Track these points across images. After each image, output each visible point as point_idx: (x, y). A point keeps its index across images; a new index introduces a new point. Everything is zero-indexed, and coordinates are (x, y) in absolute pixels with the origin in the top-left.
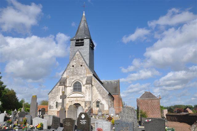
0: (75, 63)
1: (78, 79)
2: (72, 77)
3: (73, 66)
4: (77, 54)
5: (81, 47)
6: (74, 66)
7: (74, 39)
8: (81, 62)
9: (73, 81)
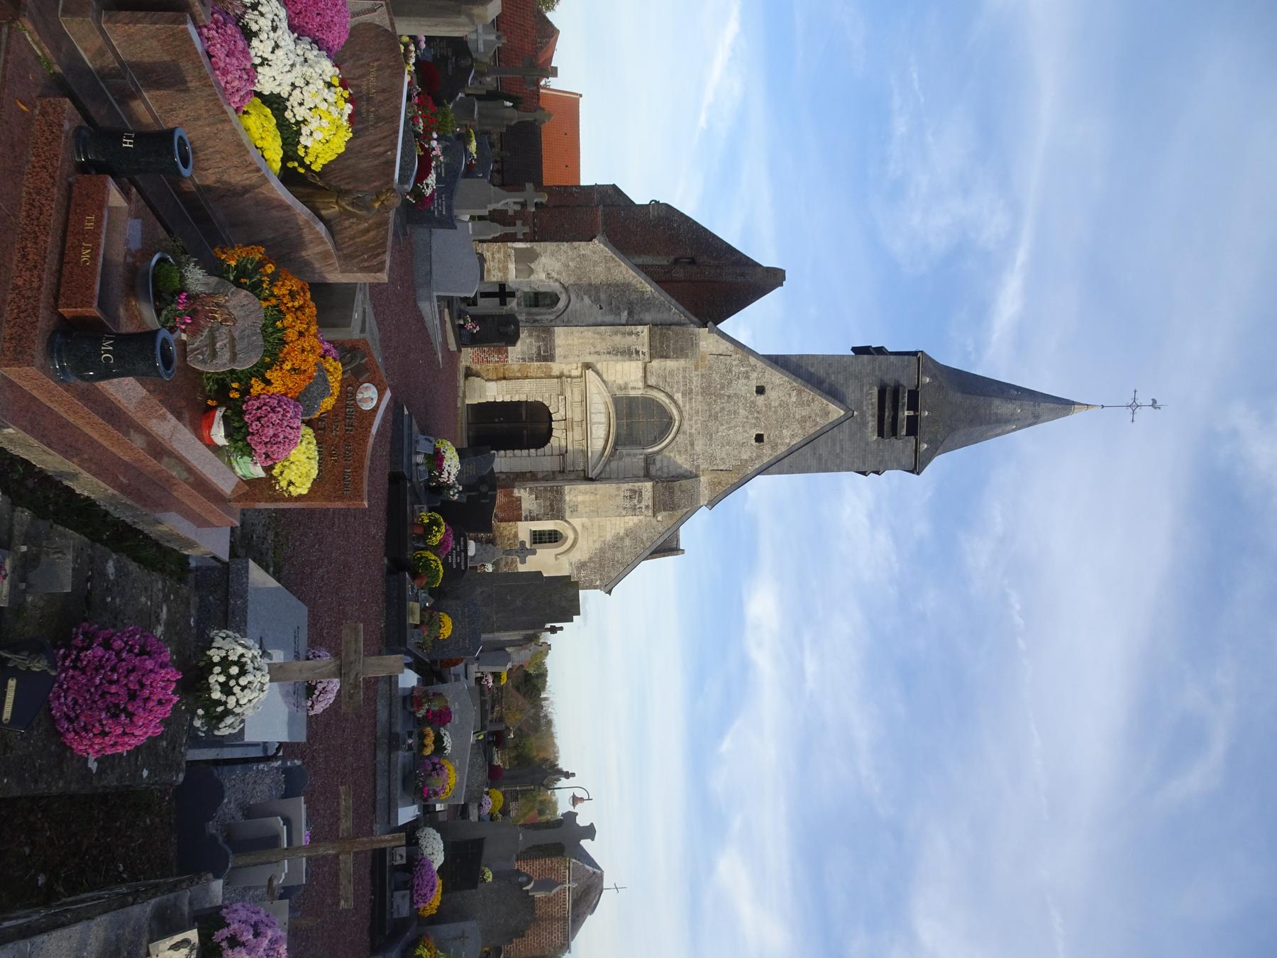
1: (686, 426)
2: (696, 383)
3: (760, 390)
4: (832, 407)
5: (872, 423)
6: (760, 400)
8: (781, 437)
9: (678, 396)
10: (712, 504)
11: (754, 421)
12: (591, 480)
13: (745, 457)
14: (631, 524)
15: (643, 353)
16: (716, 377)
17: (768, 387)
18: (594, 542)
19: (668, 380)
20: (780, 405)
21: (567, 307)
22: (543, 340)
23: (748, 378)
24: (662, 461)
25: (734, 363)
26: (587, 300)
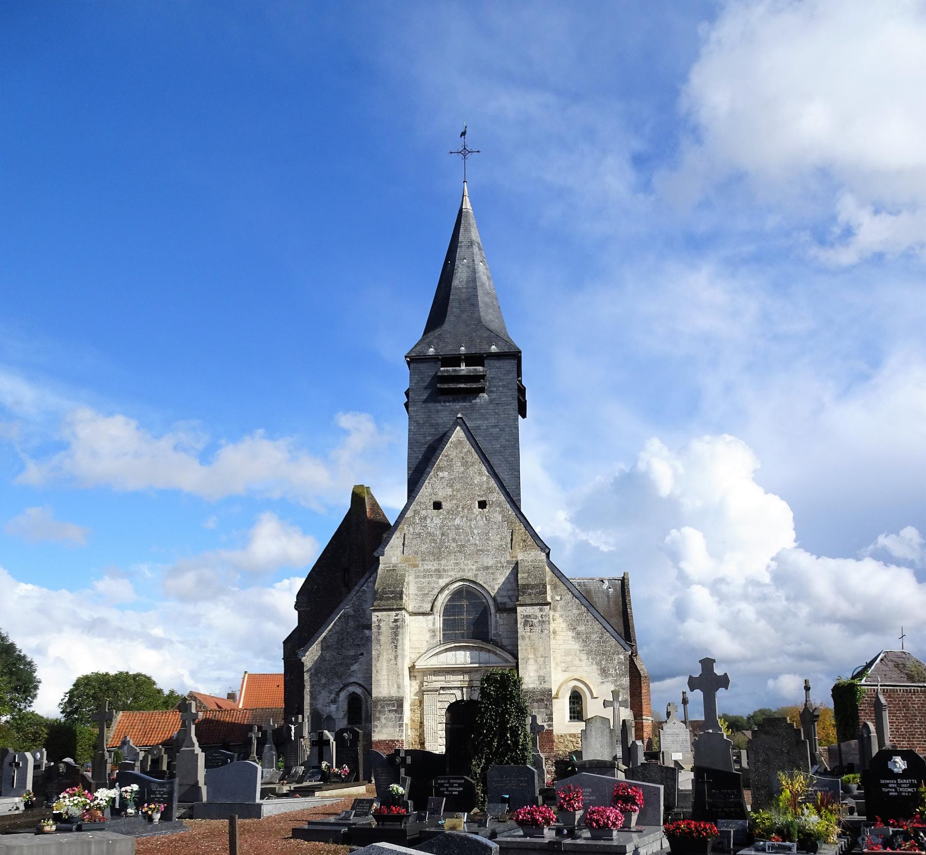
0: (449, 491)
2: (431, 565)
3: (437, 506)
4: (453, 438)
7: (431, 351)
8: (480, 485)
9: (442, 582)
11: (466, 511)
14: (564, 625)
15: (397, 615)
17: (435, 499)
18: (580, 660)
19: (426, 592)
20: (451, 486)
21: (360, 685)
22: (383, 707)
23: (425, 518)
24: (502, 596)
25: (412, 530)
26: (355, 667)
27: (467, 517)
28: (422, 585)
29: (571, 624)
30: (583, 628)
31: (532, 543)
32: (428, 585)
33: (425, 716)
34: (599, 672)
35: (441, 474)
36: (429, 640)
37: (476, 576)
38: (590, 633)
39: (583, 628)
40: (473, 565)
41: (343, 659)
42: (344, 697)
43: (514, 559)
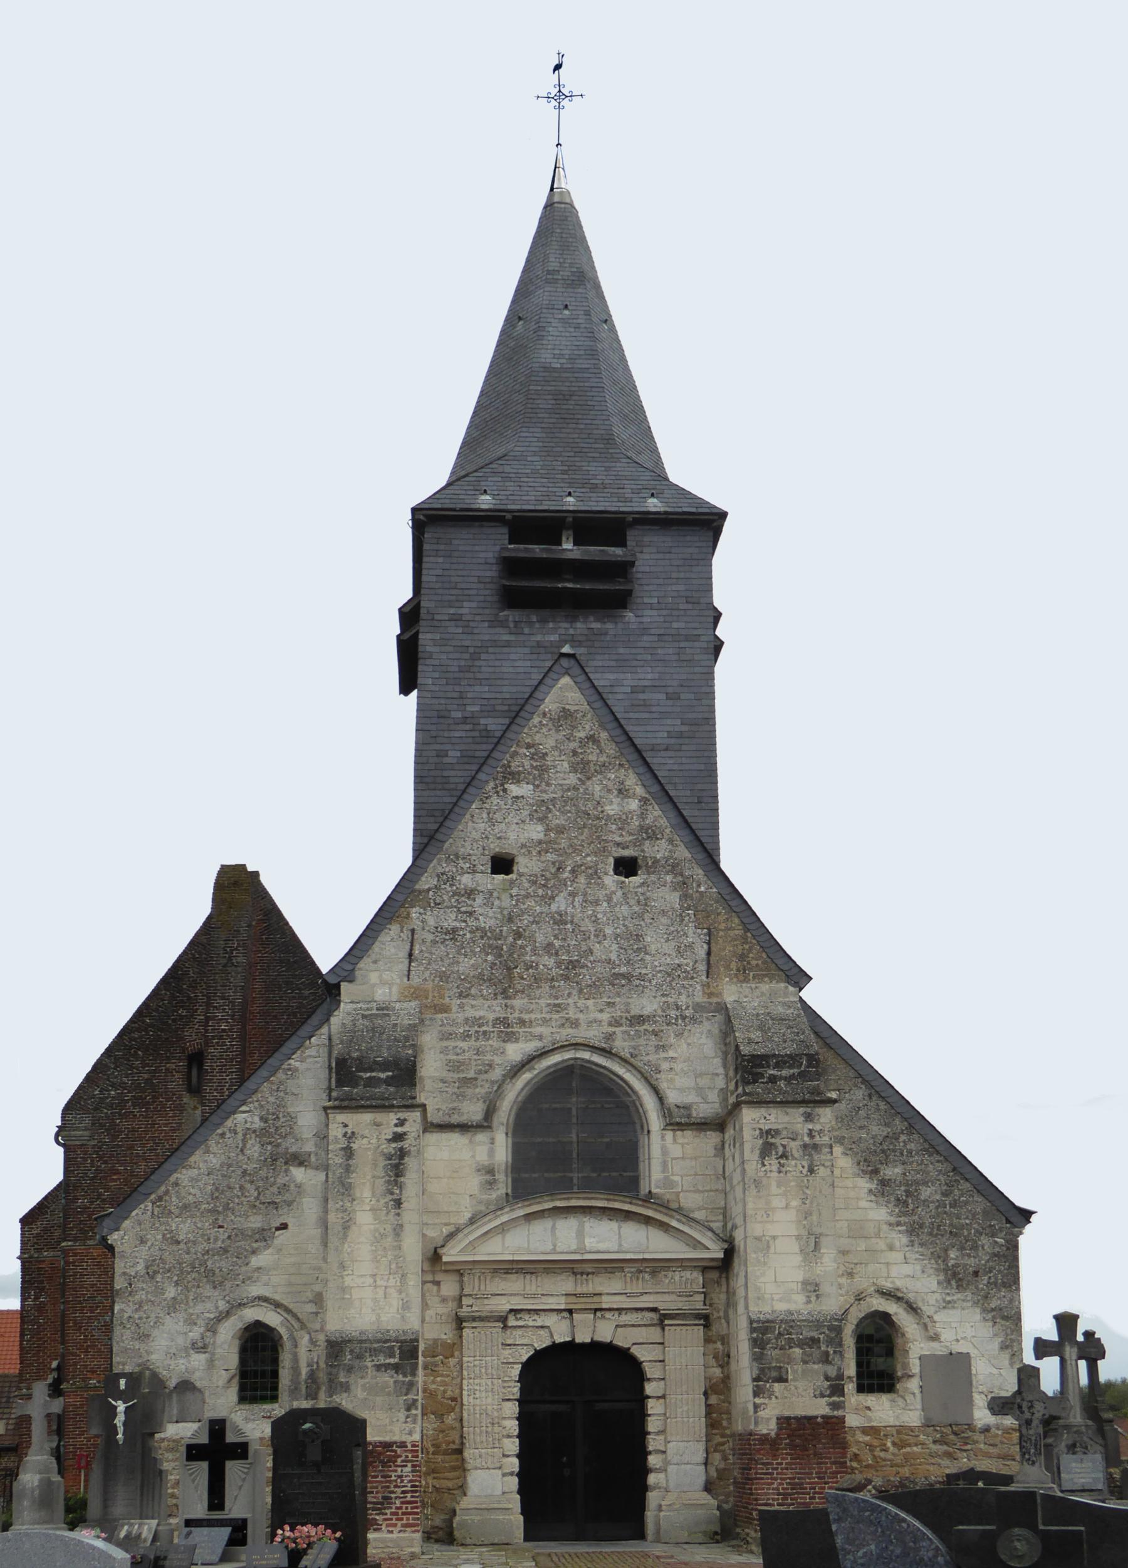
0: (536, 832)
1: (586, 1033)
2: (486, 1008)
3: (502, 864)
4: (550, 704)
8: (623, 821)
9: (515, 1052)
10: (799, 977)
11: (582, 879)
12: (730, 1253)
13: (674, 898)
16: (466, 965)
17: (495, 847)
19: (471, 1074)
21: (277, 1305)
24: (681, 1090)
26: (262, 1259)
27: (585, 894)
28: (460, 1057)
29: (865, 1160)
30: (898, 1170)
31: (764, 962)
32: (476, 1057)
33: (465, 1382)
34: (942, 1277)
35: (514, 789)
36: (476, 1192)
37: (610, 1037)
38: (917, 1183)
39: (898, 1170)
40: (601, 1011)
41: (229, 1237)
42: (231, 1334)
43: (714, 1000)
